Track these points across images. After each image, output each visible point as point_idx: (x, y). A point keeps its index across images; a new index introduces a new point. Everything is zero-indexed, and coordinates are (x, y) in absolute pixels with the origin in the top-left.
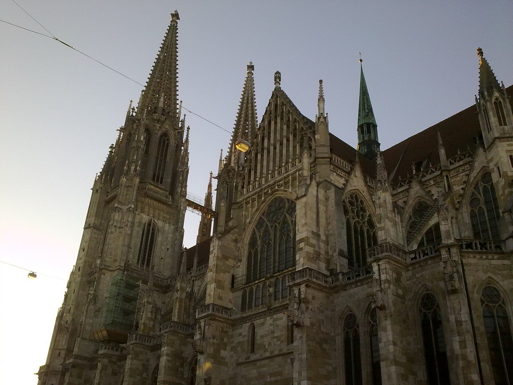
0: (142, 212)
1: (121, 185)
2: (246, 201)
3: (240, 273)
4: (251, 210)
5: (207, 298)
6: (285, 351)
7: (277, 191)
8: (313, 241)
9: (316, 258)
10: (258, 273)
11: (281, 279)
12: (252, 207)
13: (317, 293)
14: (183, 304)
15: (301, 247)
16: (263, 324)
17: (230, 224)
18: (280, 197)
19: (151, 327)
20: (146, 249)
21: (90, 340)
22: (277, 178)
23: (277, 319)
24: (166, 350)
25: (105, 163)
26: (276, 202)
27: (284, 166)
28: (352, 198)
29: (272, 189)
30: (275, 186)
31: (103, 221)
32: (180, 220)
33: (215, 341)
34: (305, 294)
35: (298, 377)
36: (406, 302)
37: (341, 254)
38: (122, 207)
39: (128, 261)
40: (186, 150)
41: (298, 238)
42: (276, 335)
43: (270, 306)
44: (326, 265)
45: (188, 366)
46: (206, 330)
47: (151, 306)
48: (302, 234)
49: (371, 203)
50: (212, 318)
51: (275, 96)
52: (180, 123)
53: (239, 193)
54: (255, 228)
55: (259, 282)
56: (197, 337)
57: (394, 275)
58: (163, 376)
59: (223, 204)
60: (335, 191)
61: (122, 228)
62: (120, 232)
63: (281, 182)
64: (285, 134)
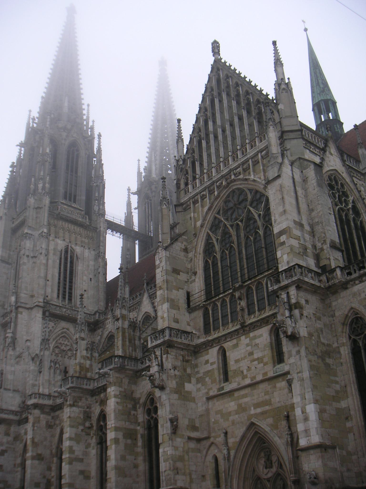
0: (56, 237)
1: (29, 207)
2: (193, 200)
3: (197, 288)
4: (202, 209)
5: (160, 321)
6: (271, 374)
7: (233, 182)
8: (297, 232)
9: (303, 253)
10: (221, 285)
11: (254, 288)
12: (203, 206)
13: (309, 297)
14: (127, 334)
15: (282, 241)
16: (236, 346)
17: (177, 231)
18: (238, 189)
19: (88, 366)
20: (65, 281)
21: (14, 390)
22: (232, 164)
23: (255, 337)
24: (113, 391)
25: (8, 185)
26: (233, 196)
27: (240, 150)
28: (330, 179)
29: (226, 180)
30: (231, 176)
31: (12, 253)
32: (101, 244)
33: (177, 372)
34: (296, 298)
35: (301, 400)
37: (333, 246)
38: (33, 233)
39: (47, 296)
40: (100, 160)
41: (276, 230)
42: (256, 356)
43: (244, 322)
44: (315, 262)
45: (141, 408)
46: (164, 360)
47: (85, 342)
48: (281, 225)
49: (352, 185)
51: (215, 70)
52: (89, 130)
53: (183, 192)
54: (209, 231)
55: (225, 296)
56: (154, 369)
58: (113, 422)
59: (165, 207)
60: (315, 170)
61: (35, 257)
62: (34, 262)
63: (238, 170)
64: (235, 111)
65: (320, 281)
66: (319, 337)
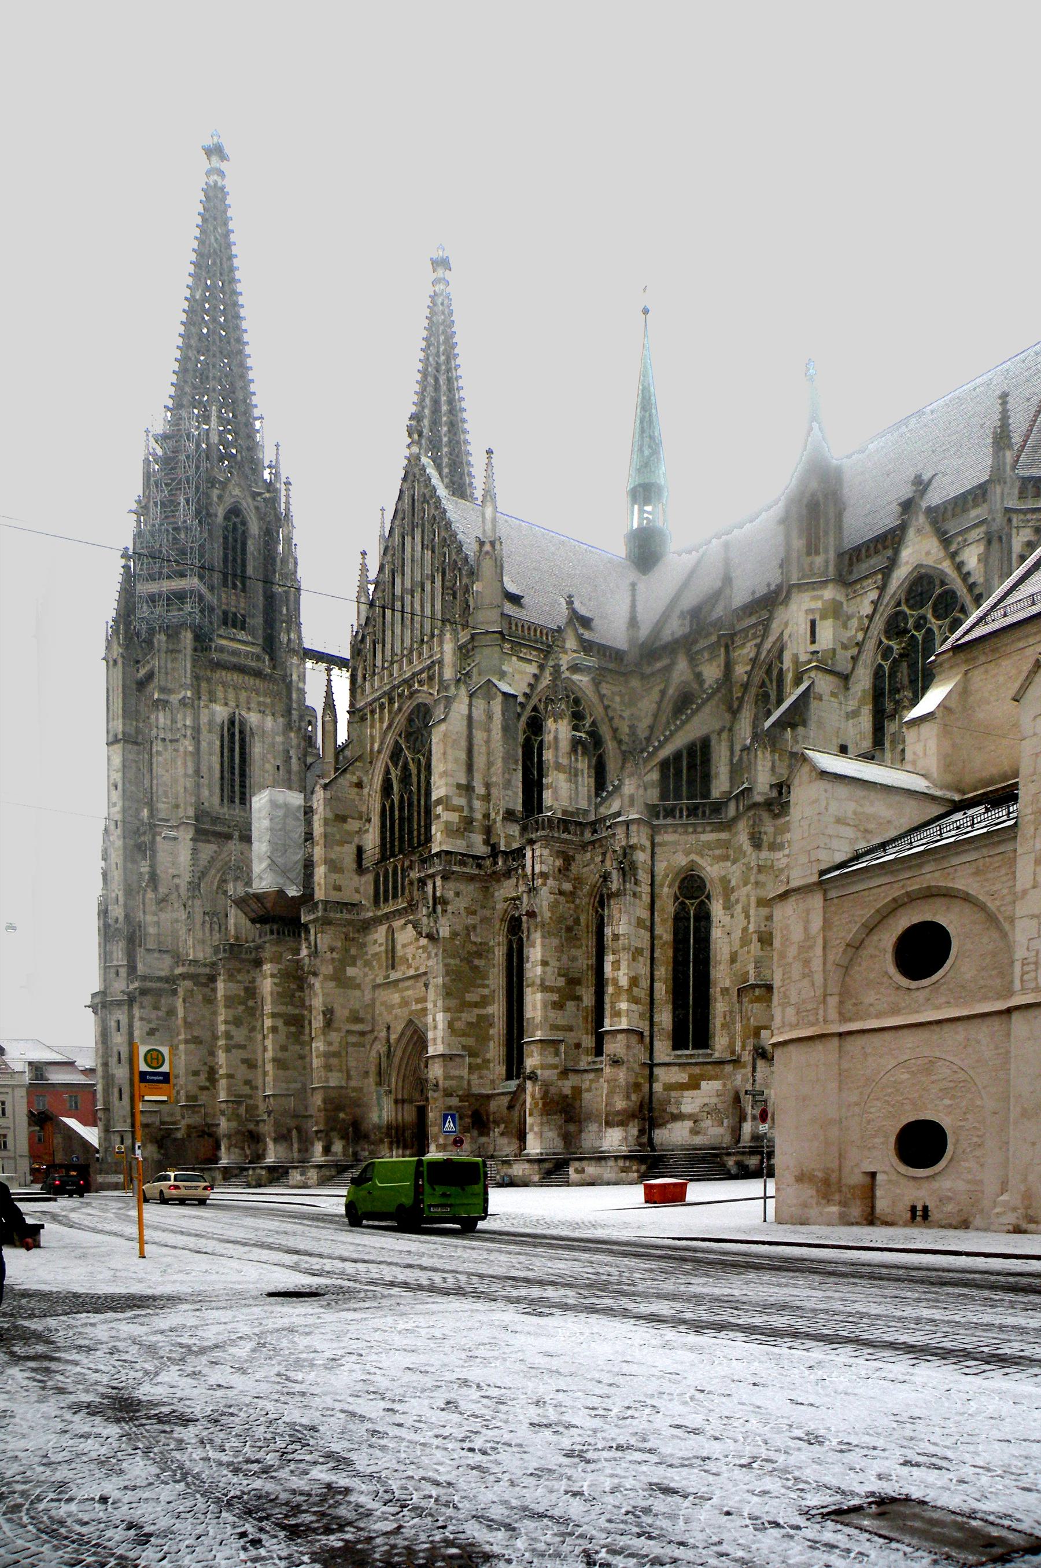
12: (381, 720)
13: (462, 887)
36: (578, 901)
37: (510, 815)
43: (412, 900)
50: (326, 922)
56: (304, 952)
57: (559, 863)
65: (479, 866)
66: (468, 935)
